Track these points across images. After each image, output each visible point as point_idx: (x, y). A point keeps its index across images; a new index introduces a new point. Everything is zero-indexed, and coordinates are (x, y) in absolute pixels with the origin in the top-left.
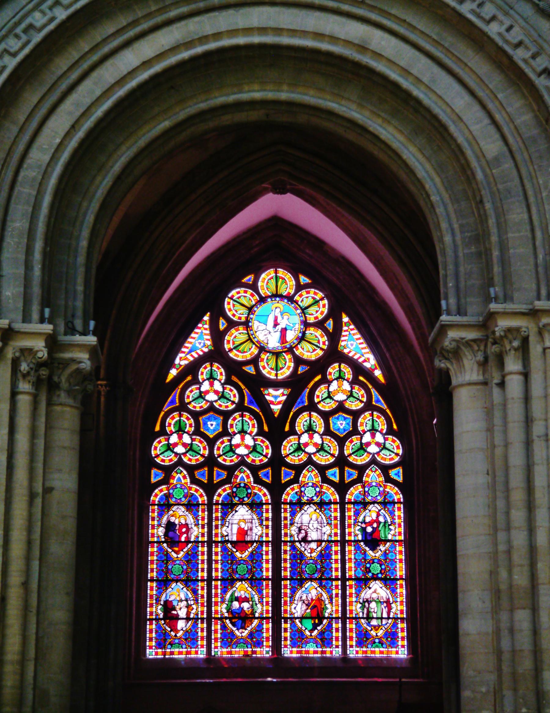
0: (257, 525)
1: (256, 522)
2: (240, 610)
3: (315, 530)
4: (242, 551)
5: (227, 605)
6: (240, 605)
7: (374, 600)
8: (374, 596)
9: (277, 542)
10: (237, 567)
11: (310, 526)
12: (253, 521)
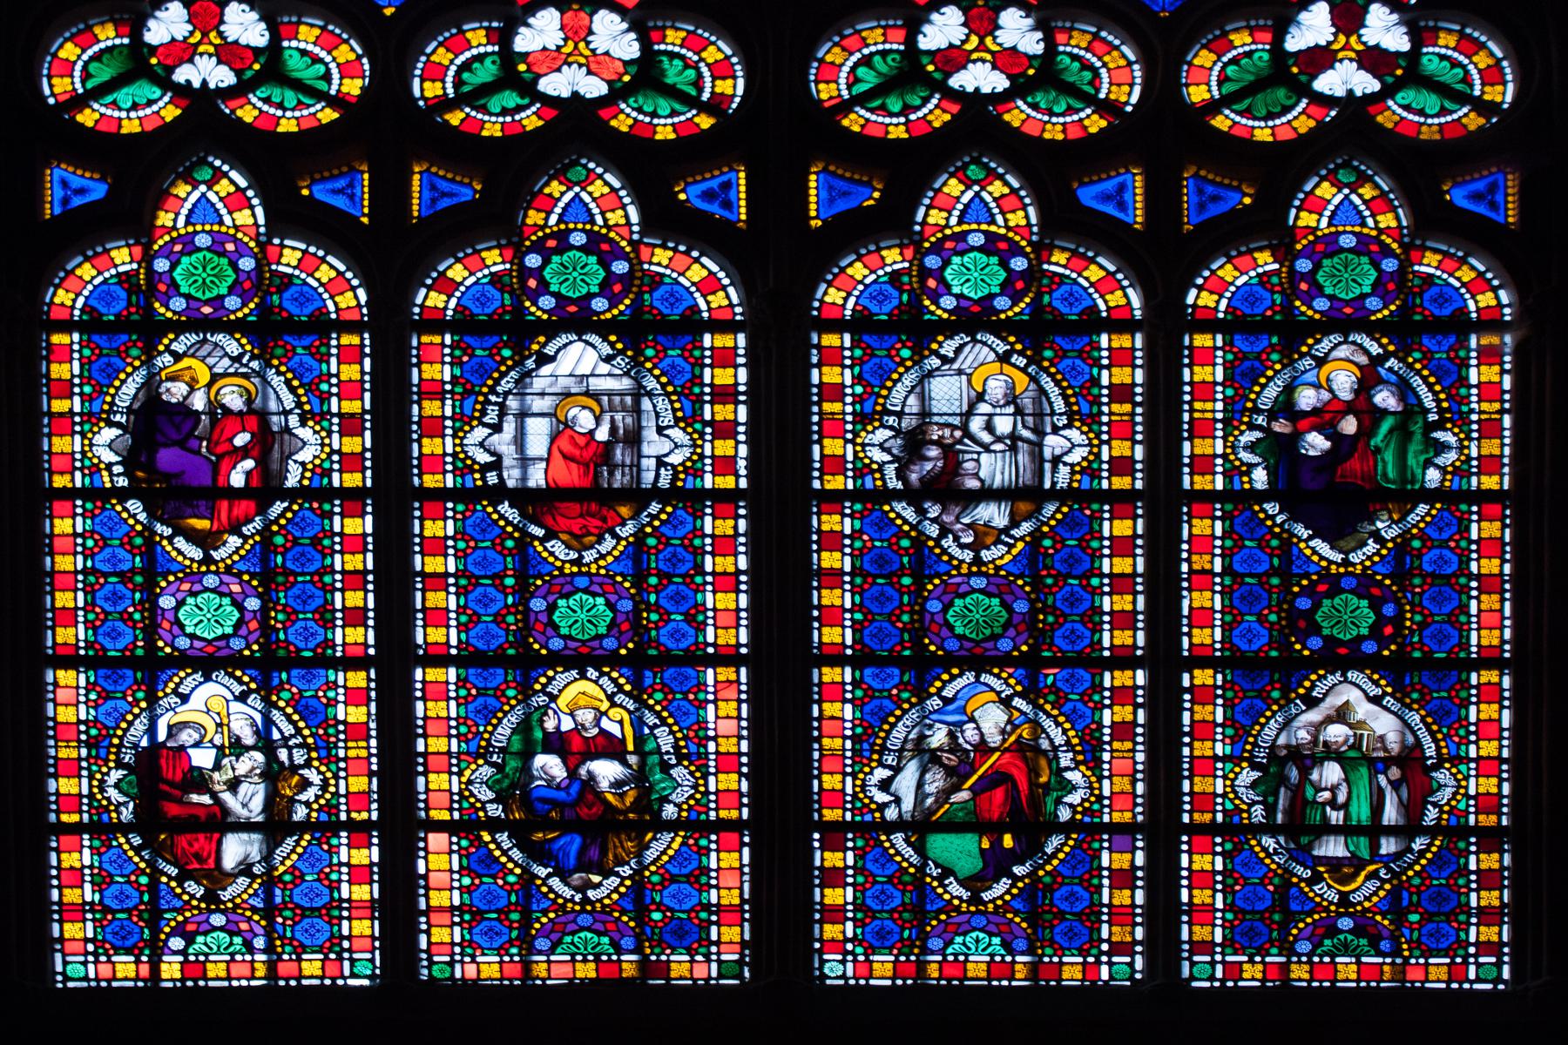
0: (667, 419)
1: (656, 409)
2: (574, 789)
3: (999, 447)
4: (578, 538)
5: (500, 768)
6: (572, 773)
7: (1331, 753)
8: (1336, 732)
9: (781, 498)
10: (552, 608)
11: (976, 425)
12: (646, 404)
